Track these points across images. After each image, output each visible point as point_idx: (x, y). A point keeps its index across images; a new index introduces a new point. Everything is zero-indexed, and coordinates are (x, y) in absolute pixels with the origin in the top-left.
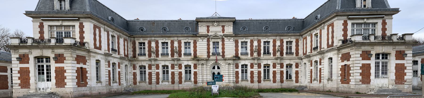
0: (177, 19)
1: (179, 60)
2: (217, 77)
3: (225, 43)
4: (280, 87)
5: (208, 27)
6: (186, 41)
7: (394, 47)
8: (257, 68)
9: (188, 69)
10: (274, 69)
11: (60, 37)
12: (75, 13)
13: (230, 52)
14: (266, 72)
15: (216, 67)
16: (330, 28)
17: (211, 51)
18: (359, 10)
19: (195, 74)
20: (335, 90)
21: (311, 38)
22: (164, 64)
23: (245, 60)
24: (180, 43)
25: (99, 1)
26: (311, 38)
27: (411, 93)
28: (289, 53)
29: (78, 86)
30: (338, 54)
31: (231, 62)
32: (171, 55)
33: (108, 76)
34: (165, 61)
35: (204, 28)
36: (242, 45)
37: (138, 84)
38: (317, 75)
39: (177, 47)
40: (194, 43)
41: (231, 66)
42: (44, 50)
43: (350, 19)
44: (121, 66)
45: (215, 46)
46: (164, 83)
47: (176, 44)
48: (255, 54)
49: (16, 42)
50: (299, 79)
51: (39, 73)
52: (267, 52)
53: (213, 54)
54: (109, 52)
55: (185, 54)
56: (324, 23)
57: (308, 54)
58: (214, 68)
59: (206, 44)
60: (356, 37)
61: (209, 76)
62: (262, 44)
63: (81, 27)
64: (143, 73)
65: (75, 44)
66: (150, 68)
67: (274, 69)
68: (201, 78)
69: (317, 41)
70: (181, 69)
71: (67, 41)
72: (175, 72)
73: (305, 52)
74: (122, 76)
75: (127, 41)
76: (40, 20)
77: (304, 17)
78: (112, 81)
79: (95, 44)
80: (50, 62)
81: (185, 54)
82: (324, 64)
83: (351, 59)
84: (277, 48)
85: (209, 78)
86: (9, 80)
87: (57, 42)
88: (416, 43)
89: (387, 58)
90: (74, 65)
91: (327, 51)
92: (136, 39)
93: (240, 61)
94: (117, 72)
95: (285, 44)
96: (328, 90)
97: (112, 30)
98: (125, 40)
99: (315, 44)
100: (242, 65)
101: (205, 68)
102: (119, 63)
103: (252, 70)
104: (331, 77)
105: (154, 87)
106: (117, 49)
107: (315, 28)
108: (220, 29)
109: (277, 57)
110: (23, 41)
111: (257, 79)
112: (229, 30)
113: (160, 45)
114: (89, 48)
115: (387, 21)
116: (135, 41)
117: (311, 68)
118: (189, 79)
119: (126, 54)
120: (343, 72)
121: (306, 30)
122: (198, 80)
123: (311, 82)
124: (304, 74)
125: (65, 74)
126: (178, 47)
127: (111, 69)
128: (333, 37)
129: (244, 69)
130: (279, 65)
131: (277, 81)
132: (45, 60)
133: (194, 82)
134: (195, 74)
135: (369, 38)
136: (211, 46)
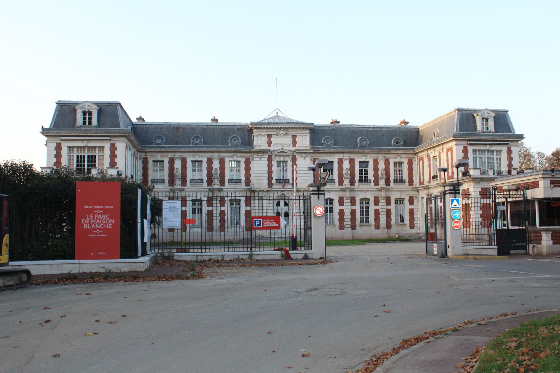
5: (269, 136)
8: (350, 204)
10: (377, 207)
14: (365, 210)
15: (282, 203)
17: (275, 176)
32: (207, 182)
39: (218, 169)
48: (346, 183)
50: (415, 222)
52: (364, 179)
58: (278, 204)
62: (357, 166)
73: (422, 181)
92: (148, 154)
103: (341, 208)
108: (289, 140)
109: (379, 187)
111: (350, 223)
112: (304, 142)
113: (189, 165)
130: (385, 201)
131: (381, 226)
136: (275, 168)
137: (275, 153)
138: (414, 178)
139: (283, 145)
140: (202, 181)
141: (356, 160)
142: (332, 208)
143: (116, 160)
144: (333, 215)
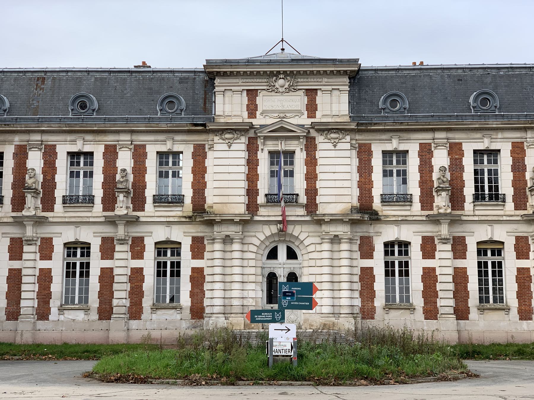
2: (286, 293)
3: (318, 154)
5: (252, 94)
6: (163, 148)
8: (450, 255)
9: (169, 259)
13: (338, 191)
15: (282, 253)
17: (264, 186)
19: (198, 277)
22: (72, 240)
23: (396, 223)
24: (139, 154)
31: (341, 230)
34: (77, 224)
35: (237, 98)
36: (384, 163)
39: (129, 170)
40: (195, 155)
41: (345, 246)
45: (276, 168)
46: (70, 315)
47: (125, 161)
48: (441, 202)
53: (272, 200)
55: (160, 200)
58: (273, 255)
59: (243, 162)
61: (252, 286)
62: (468, 162)
68: (218, 294)
70: (142, 258)
72: (116, 271)
81: (160, 200)
85: (252, 294)
100: (386, 245)
101: (237, 255)
103: (429, 263)
108: (297, 101)
111: (452, 303)
112: (335, 104)
113: (62, 163)
118: (172, 300)
122: (206, 302)
126: (134, 170)
129: (396, 259)
133: (192, 310)
134: (198, 277)
136: (264, 168)
137: (265, 133)
139: (283, 114)
140: (90, 200)
141: (465, 147)
142: (407, 263)
144: (407, 282)
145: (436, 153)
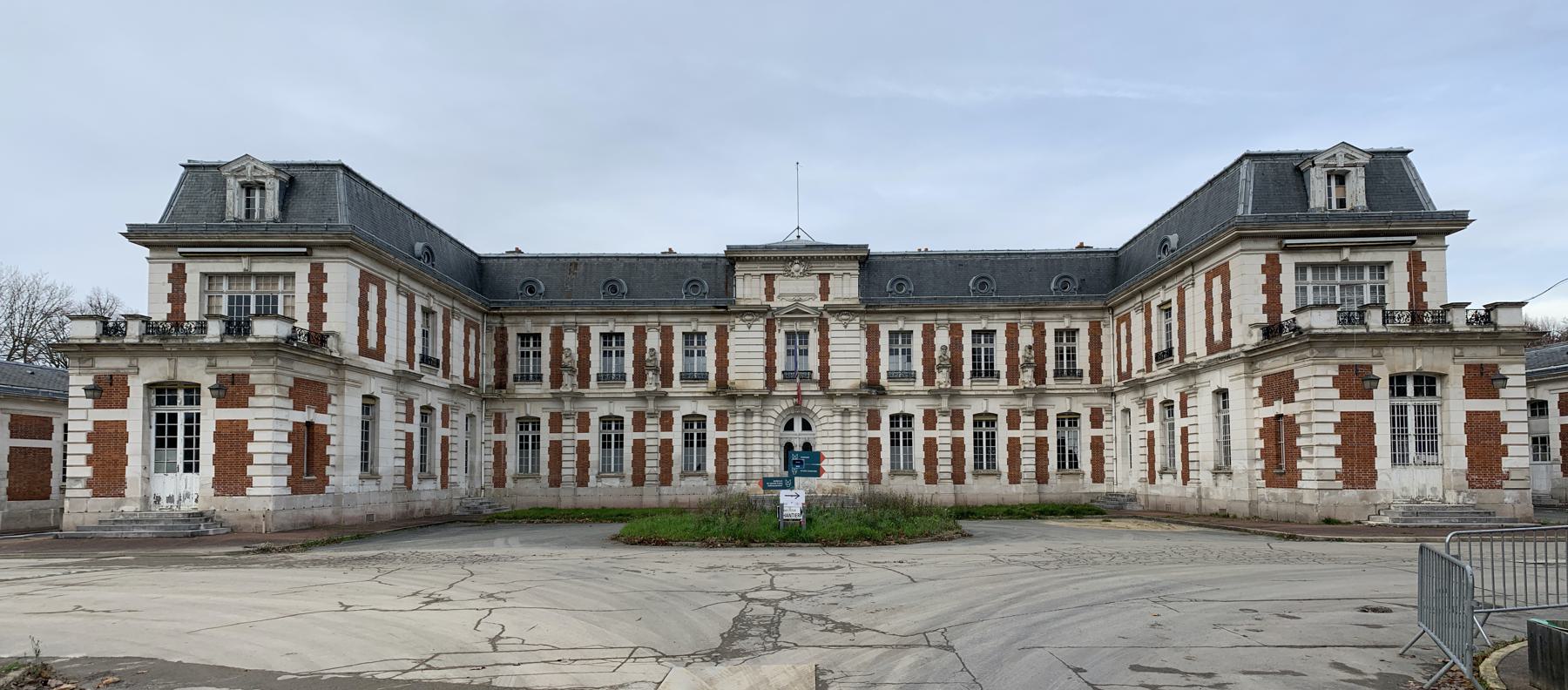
0: (657, 251)
1: (665, 397)
3: (830, 334)
4: (1034, 499)
5: (770, 278)
7: (1458, 352)
8: (949, 426)
9: (695, 431)
10: (1014, 434)
11: (239, 313)
12: (297, 230)
13: (848, 368)
15: (798, 425)
16: (1217, 281)
17: (781, 364)
18: (1323, 218)
19: (722, 446)
20: (1244, 510)
21: (1148, 318)
23: (901, 397)
24: (667, 335)
25: (385, 189)
26: (1148, 318)
27: (1528, 520)
28: (1068, 372)
29: (294, 492)
30: (1249, 376)
31: (850, 404)
33: (402, 453)
34: (611, 399)
35: (756, 281)
37: (509, 483)
38: (1173, 454)
39: (658, 350)
40: (717, 336)
41: (854, 418)
42: (180, 360)
43: (1288, 249)
44: (453, 417)
46: (607, 482)
47: (653, 341)
48: (942, 378)
49: (87, 331)
50: (1106, 467)
51: (160, 443)
53: (788, 376)
54: (412, 367)
55: (686, 377)
56: (1192, 264)
57: (1135, 375)
58: (789, 426)
60: (1315, 313)
63: (318, 278)
64: (528, 444)
65: (291, 339)
66: (556, 425)
67: (1014, 434)
69: (1169, 327)
71: (265, 329)
73: (1124, 369)
74: (454, 456)
75: (476, 327)
76: (174, 256)
77: (1117, 244)
78: (416, 473)
79: (362, 340)
80: (198, 403)
82: (1199, 411)
83: (1298, 396)
84: (1021, 354)
85: (771, 462)
86: (56, 467)
87: (228, 332)
88: (1535, 336)
89: (1432, 392)
90: (282, 414)
91: (1209, 367)
92: (507, 320)
93: (885, 401)
94: (439, 441)
95: (1050, 339)
96: (1215, 509)
97: (426, 291)
98: (468, 326)
99: (1160, 338)
100: (892, 417)
101: (756, 426)
102: (445, 407)
103: (931, 434)
104: (1228, 461)
105: (568, 496)
106: (440, 357)
107: (1161, 282)
108: (811, 285)
110: (111, 329)
111: (950, 469)
112: (846, 288)
113: (595, 343)
114: (340, 352)
115: (1426, 256)
116: (503, 329)
117: (1150, 427)
119: (472, 375)
120: (1272, 445)
121: (1128, 289)
122: (730, 470)
123: (1152, 480)
124: (1123, 449)
125: (251, 448)
127: (415, 428)
128: (1227, 315)
129: (901, 429)
130: (1032, 419)
131: (1025, 476)
132: (181, 394)
134: (722, 446)
135: (1362, 319)
136: (781, 347)
138: (1104, 366)
139: (798, 297)
141: (964, 327)
143: (326, 308)
145: (938, 333)
